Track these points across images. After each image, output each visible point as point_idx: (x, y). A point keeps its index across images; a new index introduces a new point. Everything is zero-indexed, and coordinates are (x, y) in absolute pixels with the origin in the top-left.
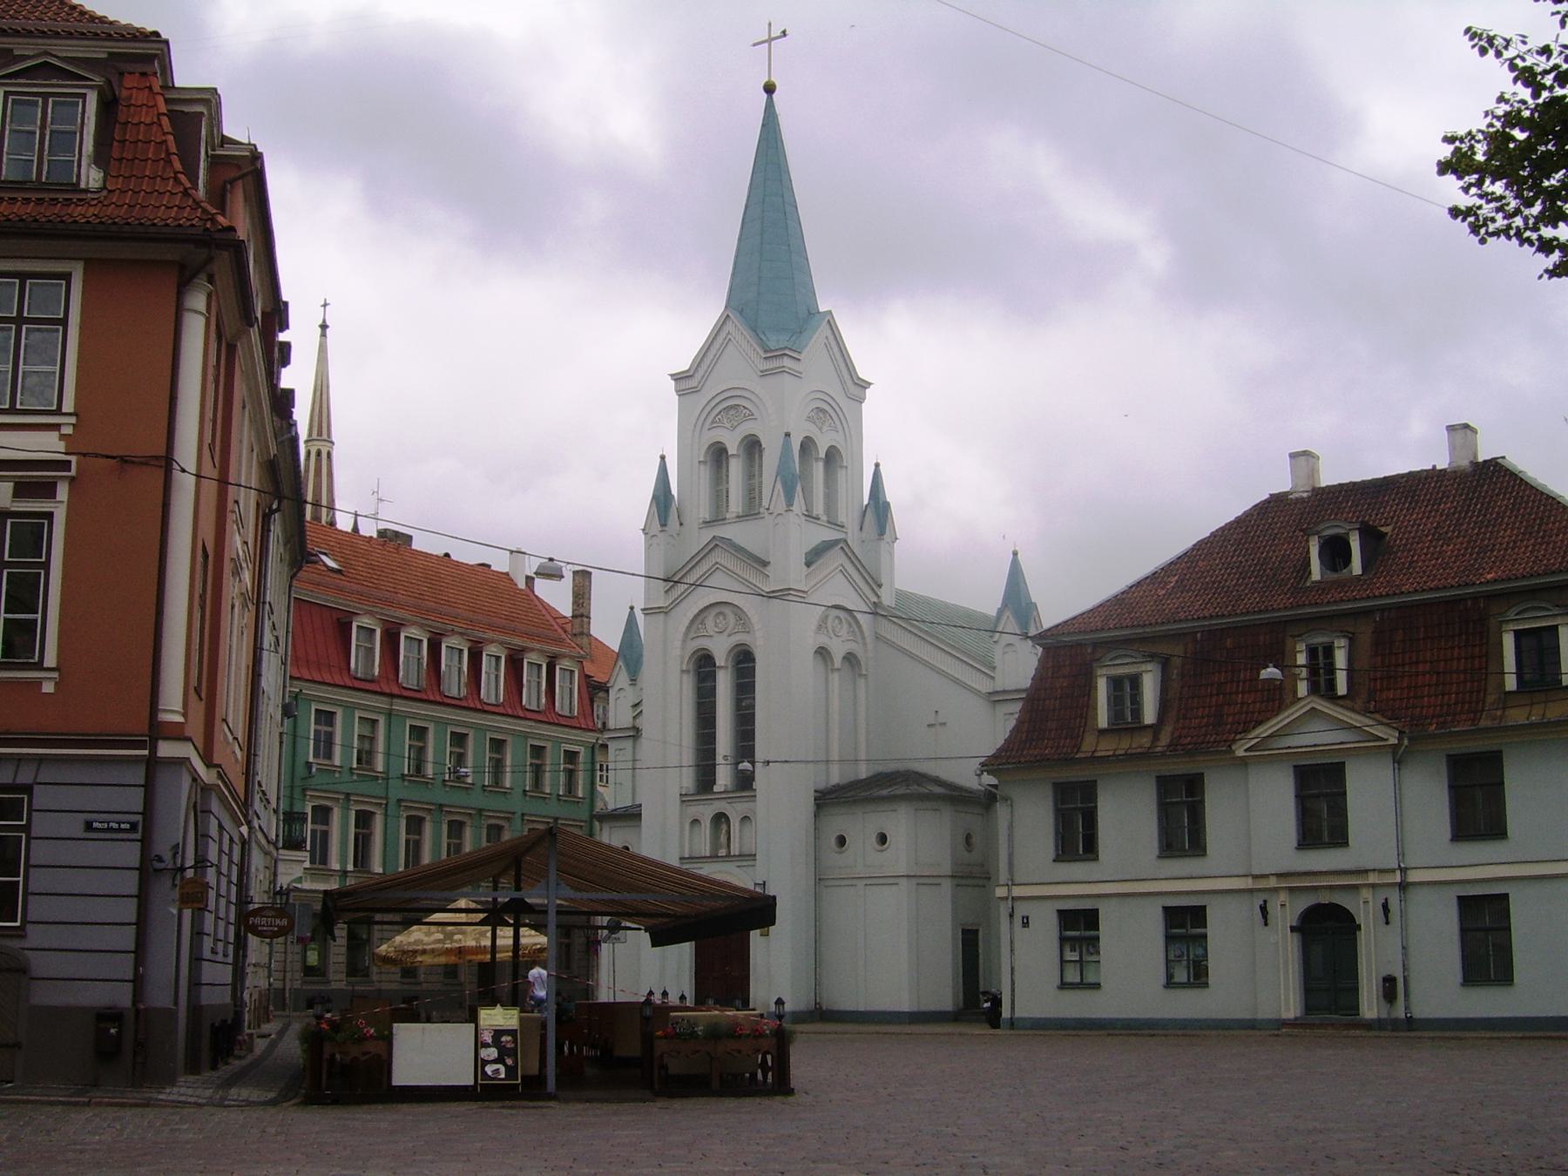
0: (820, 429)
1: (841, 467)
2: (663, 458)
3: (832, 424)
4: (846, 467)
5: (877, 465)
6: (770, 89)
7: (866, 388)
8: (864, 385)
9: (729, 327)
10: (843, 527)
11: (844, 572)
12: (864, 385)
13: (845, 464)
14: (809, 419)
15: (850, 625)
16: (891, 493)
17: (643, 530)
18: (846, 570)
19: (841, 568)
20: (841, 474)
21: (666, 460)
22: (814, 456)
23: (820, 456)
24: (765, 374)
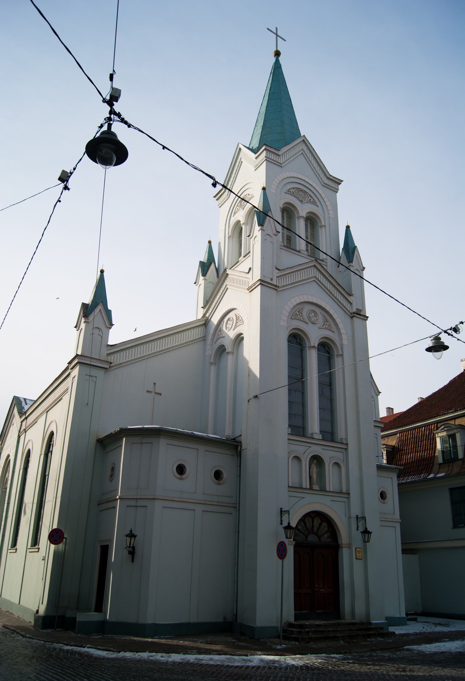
0: (301, 201)
1: (321, 226)
2: (210, 242)
3: (312, 200)
4: (325, 226)
5: (348, 227)
7: (340, 184)
8: (338, 182)
11: (317, 281)
12: (338, 182)
13: (323, 224)
16: (357, 241)
18: (318, 279)
19: (314, 279)
21: (212, 243)
22: (296, 216)
23: (301, 215)
24: (257, 168)
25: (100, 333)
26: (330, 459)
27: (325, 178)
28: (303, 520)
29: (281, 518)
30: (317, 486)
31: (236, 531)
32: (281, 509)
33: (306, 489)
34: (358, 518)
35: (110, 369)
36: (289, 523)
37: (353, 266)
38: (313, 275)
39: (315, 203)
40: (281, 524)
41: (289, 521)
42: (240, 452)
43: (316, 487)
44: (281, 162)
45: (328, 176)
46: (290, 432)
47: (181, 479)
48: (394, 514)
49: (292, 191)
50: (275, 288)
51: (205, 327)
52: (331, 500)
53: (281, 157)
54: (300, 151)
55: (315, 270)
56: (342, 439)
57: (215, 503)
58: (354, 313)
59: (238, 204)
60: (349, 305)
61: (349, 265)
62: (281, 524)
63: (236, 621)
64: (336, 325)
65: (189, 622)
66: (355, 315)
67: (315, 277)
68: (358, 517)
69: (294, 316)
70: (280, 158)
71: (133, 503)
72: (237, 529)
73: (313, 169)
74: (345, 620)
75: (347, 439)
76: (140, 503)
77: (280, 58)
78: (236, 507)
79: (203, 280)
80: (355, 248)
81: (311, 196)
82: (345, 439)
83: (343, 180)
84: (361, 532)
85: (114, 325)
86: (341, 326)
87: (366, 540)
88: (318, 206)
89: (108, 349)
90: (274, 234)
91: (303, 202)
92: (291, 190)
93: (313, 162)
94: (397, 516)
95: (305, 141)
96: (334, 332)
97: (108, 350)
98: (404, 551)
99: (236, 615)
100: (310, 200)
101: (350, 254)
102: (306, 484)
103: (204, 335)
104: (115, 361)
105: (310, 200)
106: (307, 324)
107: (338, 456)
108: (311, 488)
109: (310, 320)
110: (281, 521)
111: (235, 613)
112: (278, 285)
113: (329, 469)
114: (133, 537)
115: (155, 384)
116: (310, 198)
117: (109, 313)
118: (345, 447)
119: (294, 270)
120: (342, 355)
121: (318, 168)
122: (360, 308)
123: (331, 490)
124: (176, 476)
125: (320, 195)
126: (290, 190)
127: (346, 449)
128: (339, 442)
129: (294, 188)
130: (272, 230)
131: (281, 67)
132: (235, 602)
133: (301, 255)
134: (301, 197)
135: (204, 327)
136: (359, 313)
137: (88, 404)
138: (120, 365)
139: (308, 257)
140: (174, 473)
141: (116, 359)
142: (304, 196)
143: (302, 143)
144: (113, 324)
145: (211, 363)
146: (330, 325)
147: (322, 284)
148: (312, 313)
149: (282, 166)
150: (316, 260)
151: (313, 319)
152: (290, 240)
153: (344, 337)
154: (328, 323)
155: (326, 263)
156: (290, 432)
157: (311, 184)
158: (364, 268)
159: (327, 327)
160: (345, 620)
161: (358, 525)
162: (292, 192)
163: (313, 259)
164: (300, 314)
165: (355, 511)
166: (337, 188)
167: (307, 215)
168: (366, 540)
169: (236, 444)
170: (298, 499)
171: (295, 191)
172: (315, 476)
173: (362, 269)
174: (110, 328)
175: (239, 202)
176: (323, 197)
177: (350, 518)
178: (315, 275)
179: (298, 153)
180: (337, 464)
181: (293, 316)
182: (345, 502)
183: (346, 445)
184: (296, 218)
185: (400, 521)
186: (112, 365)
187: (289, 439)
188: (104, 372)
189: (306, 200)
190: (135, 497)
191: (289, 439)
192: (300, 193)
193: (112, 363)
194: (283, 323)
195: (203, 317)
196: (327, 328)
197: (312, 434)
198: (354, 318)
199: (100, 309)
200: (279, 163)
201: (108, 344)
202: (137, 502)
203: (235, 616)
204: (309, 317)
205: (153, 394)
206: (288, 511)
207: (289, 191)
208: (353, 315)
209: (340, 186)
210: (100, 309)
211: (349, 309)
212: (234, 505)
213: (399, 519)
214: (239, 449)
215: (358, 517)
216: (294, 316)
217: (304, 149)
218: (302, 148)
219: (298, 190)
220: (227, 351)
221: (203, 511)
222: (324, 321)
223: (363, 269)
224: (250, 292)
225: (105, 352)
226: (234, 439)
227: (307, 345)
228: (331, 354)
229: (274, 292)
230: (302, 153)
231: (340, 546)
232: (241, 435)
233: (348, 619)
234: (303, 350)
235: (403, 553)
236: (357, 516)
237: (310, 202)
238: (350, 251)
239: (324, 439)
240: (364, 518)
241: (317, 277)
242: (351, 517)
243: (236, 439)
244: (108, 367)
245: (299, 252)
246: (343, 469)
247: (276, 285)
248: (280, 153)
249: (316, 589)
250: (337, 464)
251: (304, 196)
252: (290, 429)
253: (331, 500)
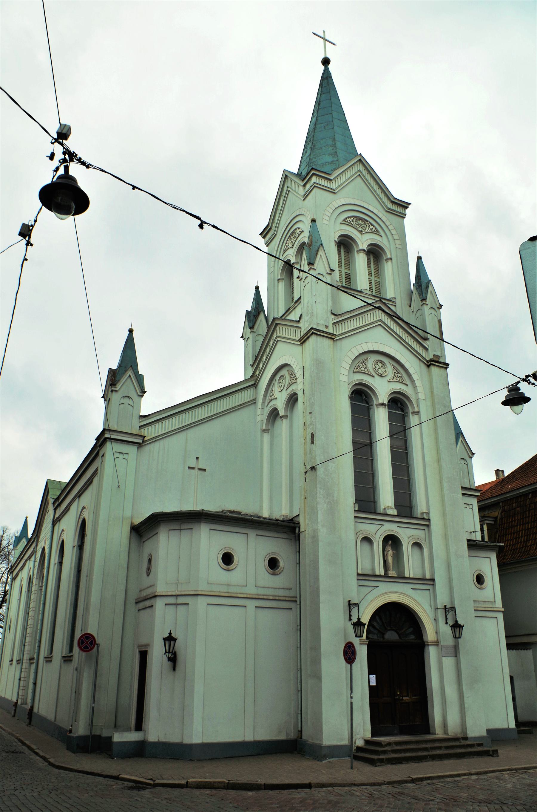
0: (361, 232)
2: (257, 288)
4: (391, 259)
5: (419, 258)
6: (326, 62)
7: (407, 208)
8: (405, 205)
9: (288, 183)
12: (405, 205)
14: (345, 222)
15: (394, 367)
16: (431, 273)
17: (242, 337)
18: (384, 323)
20: (388, 269)
23: (361, 247)
24: (305, 196)
25: (131, 403)
26: (408, 538)
27: (389, 202)
29: (350, 612)
30: (394, 572)
31: (297, 629)
32: (349, 601)
33: (380, 576)
34: (447, 608)
35: (144, 444)
36: (359, 619)
37: (427, 304)
38: (378, 319)
40: (350, 620)
41: (359, 616)
42: (299, 535)
43: (392, 573)
44: (334, 188)
45: (393, 200)
46: (357, 509)
47: (228, 570)
48: (495, 602)
49: (349, 220)
50: (332, 337)
51: (256, 388)
52: (412, 589)
53: (334, 181)
54: (356, 173)
55: (380, 312)
56: (422, 513)
57: (271, 598)
58: (431, 360)
59: (287, 240)
60: (424, 351)
61: (423, 303)
62: (350, 620)
63: (301, 738)
64: (409, 375)
65: (244, 740)
66: (432, 363)
67: (381, 321)
68: (447, 607)
69: (357, 368)
70: (332, 182)
71: (172, 600)
72: (299, 628)
73: (373, 192)
74: (435, 734)
75: (428, 513)
76: (181, 600)
77: (330, 67)
78: (296, 601)
79: (250, 333)
80: (429, 282)
81: (372, 225)
82: (426, 513)
83: (410, 203)
84: (450, 626)
85: (146, 392)
86: (415, 377)
87: (457, 636)
88: (382, 236)
89: (140, 420)
90: (328, 273)
91: (362, 233)
92: (348, 220)
93: (373, 184)
94: (499, 604)
95: (362, 161)
96: (407, 385)
97: (140, 422)
98: (510, 646)
99: (301, 731)
100: (372, 229)
101: (424, 291)
102: (380, 570)
103: (254, 398)
104: (149, 434)
105: (372, 229)
106: (374, 377)
107: (418, 534)
108: (386, 576)
109: (377, 373)
110: (350, 615)
111: (300, 729)
112: (335, 333)
114: (173, 640)
115: (197, 458)
116: (371, 227)
117: (140, 379)
118: (427, 523)
119: (354, 314)
120: (418, 412)
121: (379, 191)
122: (439, 354)
123: (412, 576)
124: (222, 566)
125: (384, 222)
126: (346, 220)
127: (428, 526)
128: (419, 517)
129: (351, 217)
130: (325, 269)
131: (331, 77)
132: (299, 715)
133: (362, 295)
134: (360, 227)
135: (254, 388)
136: (436, 360)
137: (119, 486)
138: (156, 439)
139: (372, 297)
140: (220, 563)
141: (150, 432)
142: (364, 225)
143: (358, 163)
144: (146, 391)
145: (264, 431)
146: (401, 377)
147: (390, 328)
148: (379, 364)
149: (336, 192)
150: (380, 300)
151: (380, 371)
152: (350, 279)
153: (420, 389)
154: (399, 375)
155: (395, 302)
156: (357, 509)
157: (372, 210)
158: (441, 306)
159: (398, 379)
160: (435, 734)
161: (447, 617)
162: (349, 222)
163: (378, 299)
164: (365, 366)
165: (442, 599)
166: (404, 213)
167: (369, 248)
168: (457, 636)
169: (293, 525)
170: (370, 589)
171: (352, 220)
172: (390, 559)
173: (438, 307)
174: (142, 396)
175: (288, 238)
176: (387, 225)
177: (436, 609)
178: (380, 318)
179: (354, 175)
180: (417, 545)
181: (356, 368)
182: (429, 590)
183: (428, 521)
184: (356, 252)
185: (503, 610)
186: (146, 439)
187: (355, 517)
188: (136, 447)
189: (367, 229)
190: (174, 593)
191: (355, 517)
192: (358, 221)
193: (145, 437)
194: (344, 378)
195: (252, 376)
196: (398, 381)
197: (385, 509)
198: (432, 368)
199: (130, 375)
200: (331, 189)
201: (141, 414)
202: (177, 599)
203: (299, 732)
204: (375, 369)
205: (196, 470)
206: (357, 603)
207: (346, 221)
208: (429, 363)
209: (408, 211)
210: (130, 375)
211: (424, 356)
212: (294, 599)
213: (501, 608)
214: (297, 531)
215: (447, 607)
216: (357, 368)
217: (361, 170)
218: (358, 169)
219: (356, 218)
220: (280, 416)
221: (256, 607)
222: (395, 373)
223: (440, 307)
224: (302, 343)
225: (137, 424)
226: (292, 520)
227: (375, 402)
228: (405, 412)
229: (330, 342)
230: (359, 175)
231: (426, 644)
232: (299, 515)
233: (439, 733)
234: (370, 409)
235: (508, 648)
236: (445, 606)
237: (371, 232)
238: (423, 286)
240: (453, 609)
241: (383, 320)
242: (437, 608)
243: (294, 519)
244: (141, 441)
245: (360, 292)
247: (332, 333)
248: (332, 178)
249: (398, 698)
251: (364, 225)
252: (357, 505)
253: (412, 589)
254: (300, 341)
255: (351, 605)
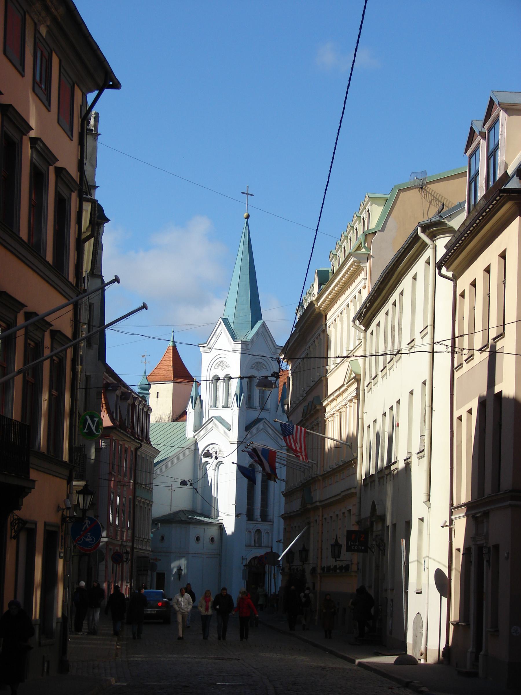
10: (268, 410)
27: (274, 348)
28: (250, 561)
33: (253, 546)
39: (267, 369)
40: (242, 564)
47: (198, 543)
62: (242, 564)
81: (264, 365)
102: (253, 544)
108: (255, 546)
110: (242, 562)
113: (264, 536)
127: (272, 525)
180: (268, 532)
189: (262, 368)
239: (262, 521)
246: (270, 534)
250: (268, 532)
254: (230, 442)
255: (242, 558)
